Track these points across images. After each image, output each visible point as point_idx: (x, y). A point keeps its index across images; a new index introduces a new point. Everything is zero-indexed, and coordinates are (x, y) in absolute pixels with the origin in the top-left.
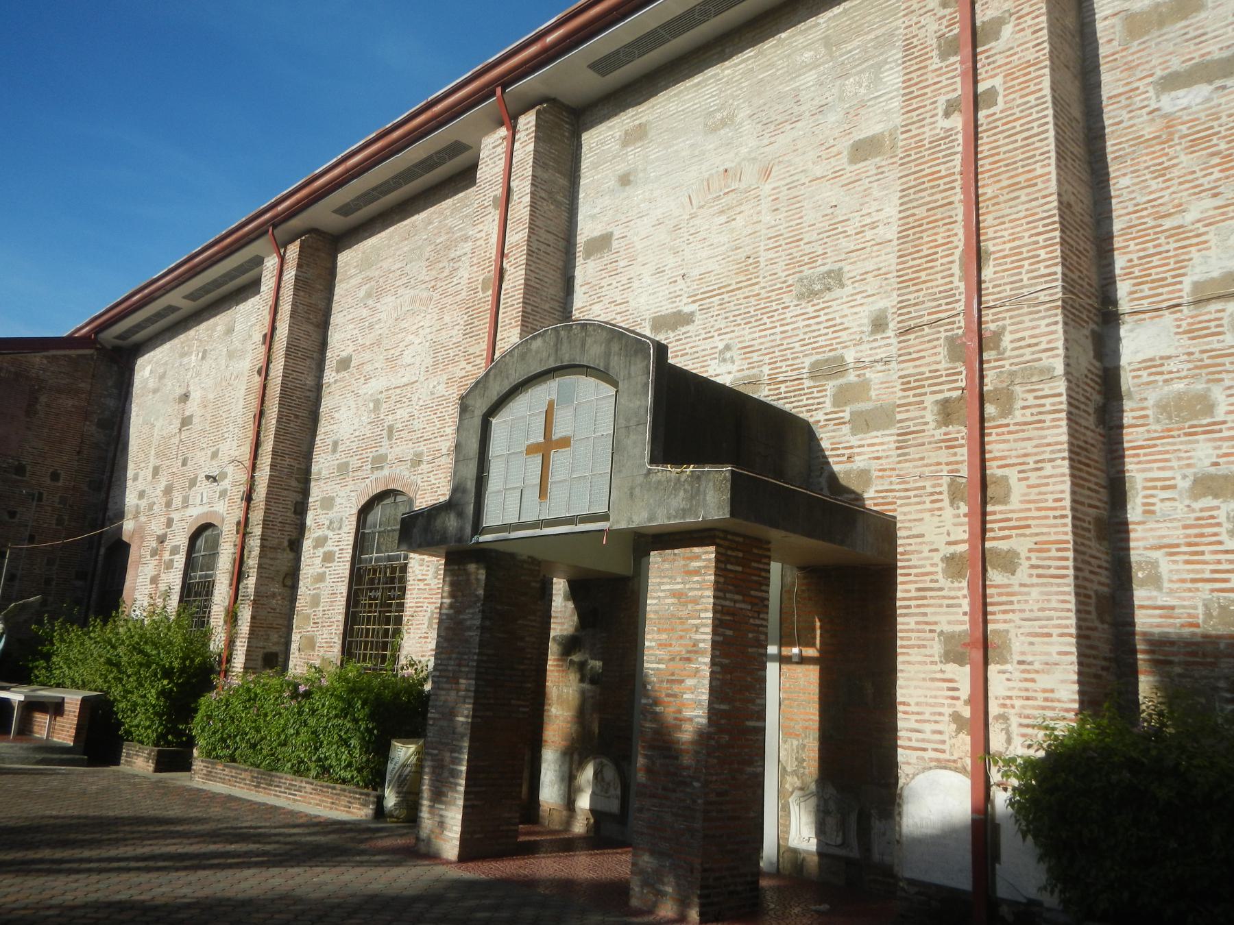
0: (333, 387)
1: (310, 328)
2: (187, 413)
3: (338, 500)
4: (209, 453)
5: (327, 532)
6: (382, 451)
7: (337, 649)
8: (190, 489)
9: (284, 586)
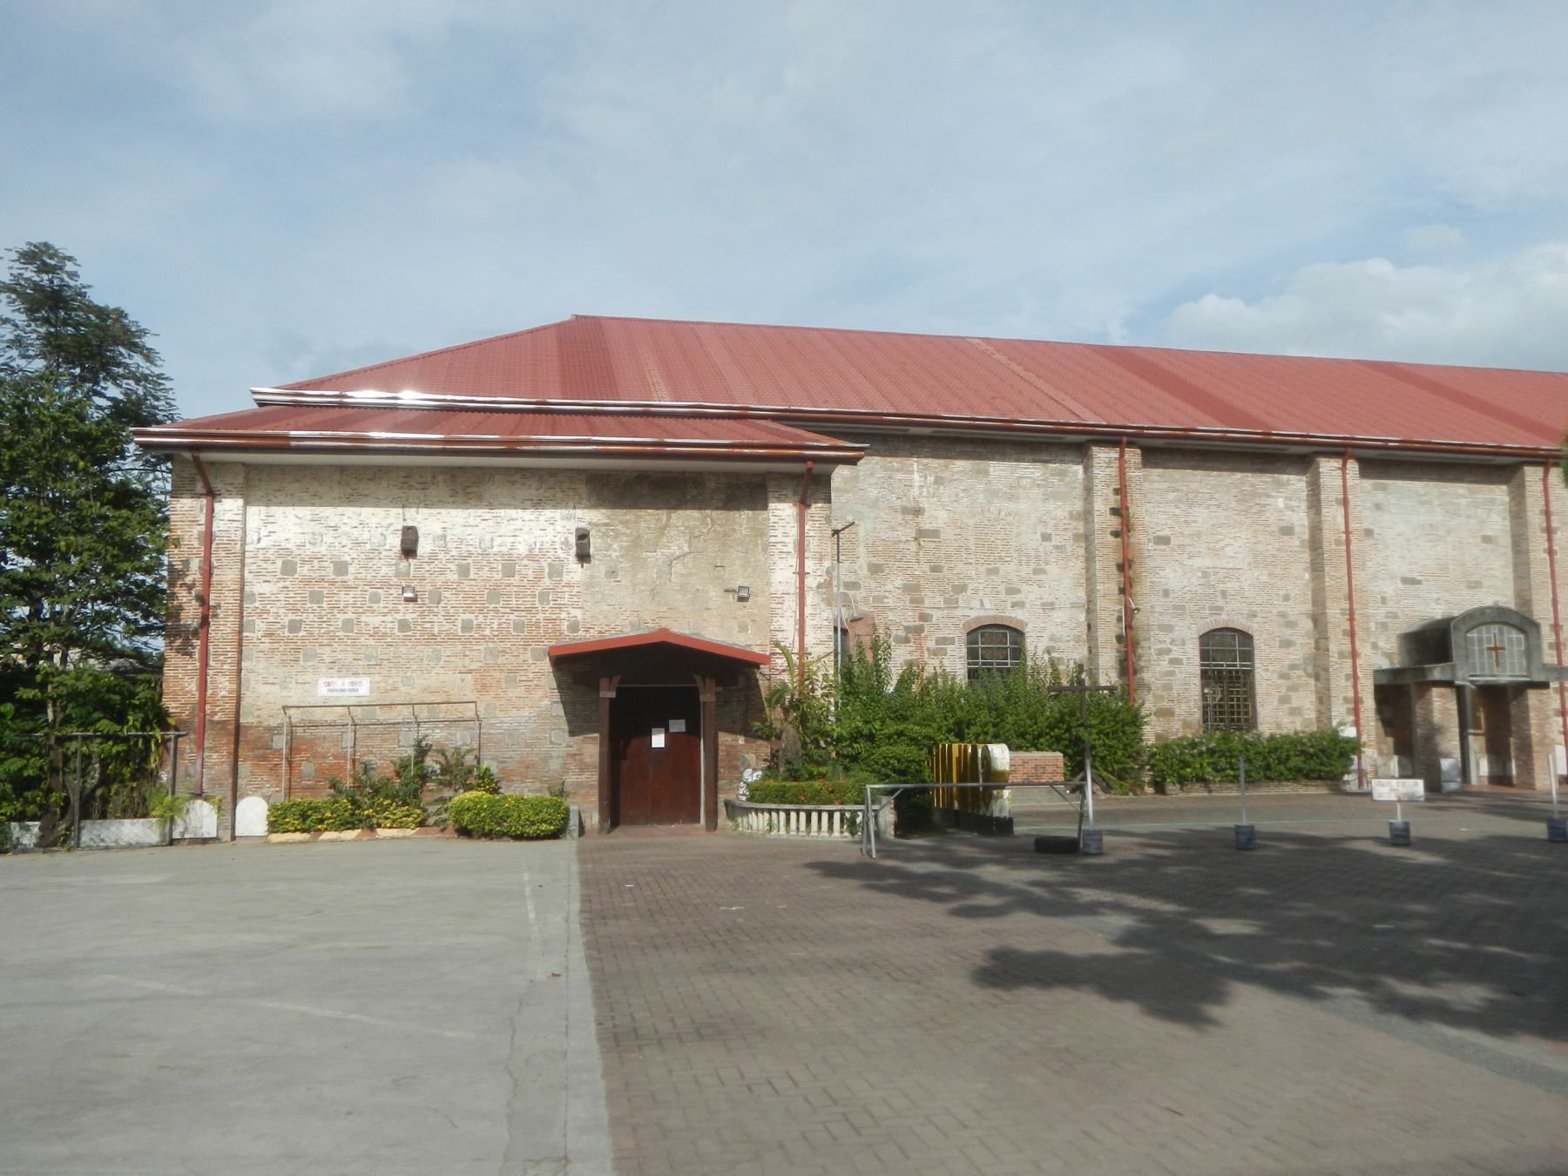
3: (1177, 628)
4: (982, 569)
5: (1170, 646)
6: (1219, 604)
7: (1197, 715)
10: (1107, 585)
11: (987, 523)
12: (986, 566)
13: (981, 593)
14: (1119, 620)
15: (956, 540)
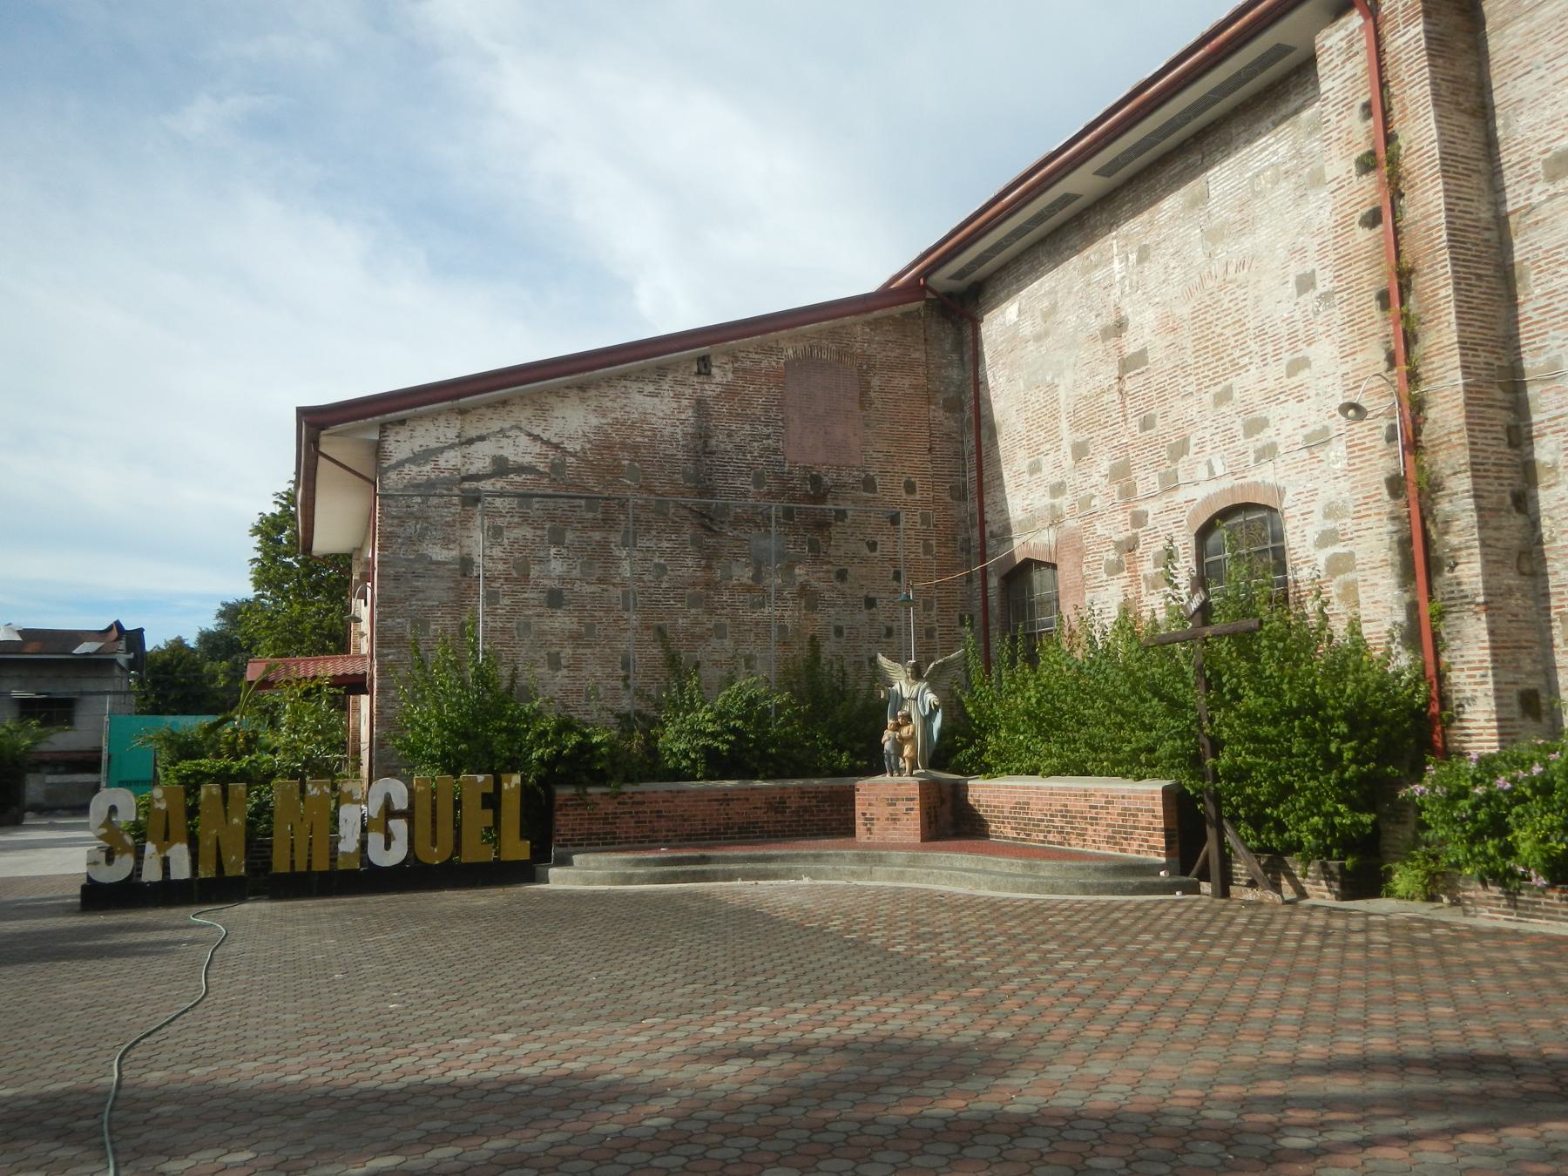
0: (1545, 211)
1: (1464, 120)
2: (1130, 350)
4: (1208, 398)
8: (1175, 460)
9: (1522, 574)
10: (1360, 357)
11: (1208, 303)
12: (1213, 390)
13: (1208, 449)
14: (1391, 438)
15: (1167, 357)
